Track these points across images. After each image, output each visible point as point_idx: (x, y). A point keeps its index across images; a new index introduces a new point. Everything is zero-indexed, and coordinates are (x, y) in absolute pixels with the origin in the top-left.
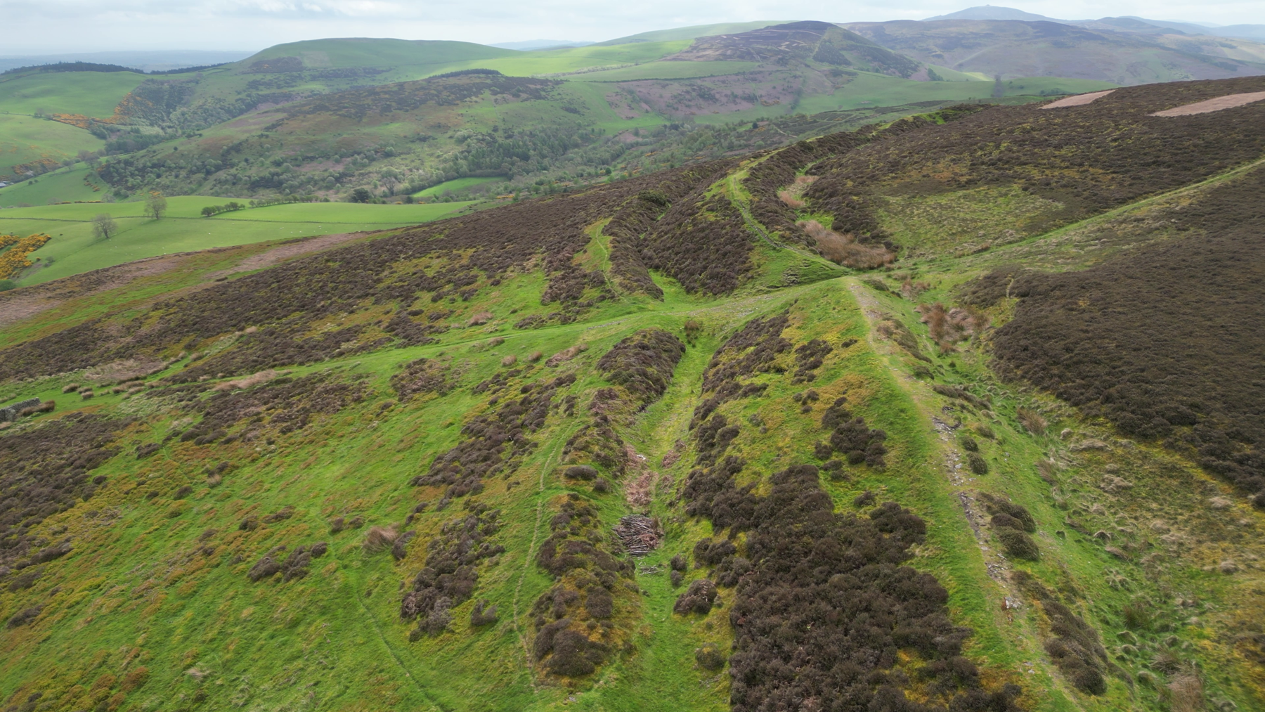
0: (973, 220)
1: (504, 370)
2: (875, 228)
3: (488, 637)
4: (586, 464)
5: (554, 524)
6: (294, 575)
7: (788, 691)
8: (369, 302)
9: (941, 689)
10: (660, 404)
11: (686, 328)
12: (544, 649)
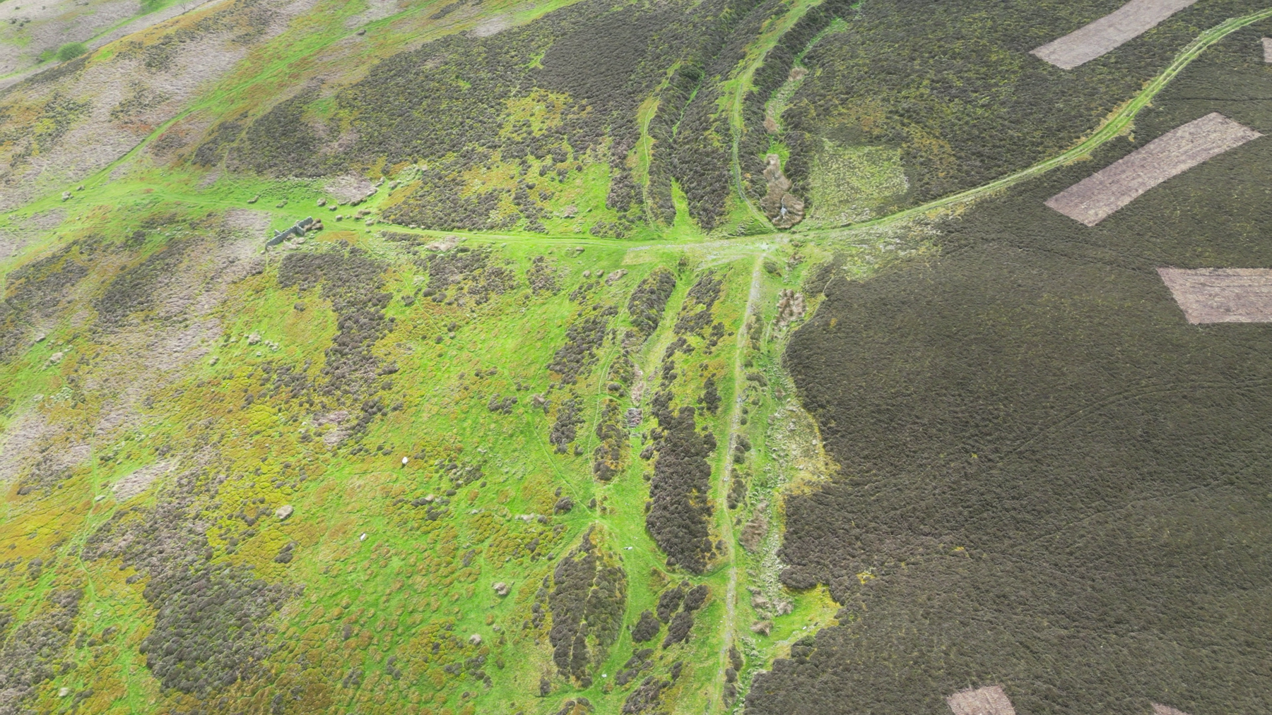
0: (857, 191)
1: (585, 280)
2: (806, 177)
3: (580, 459)
4: (616, 383)
5: (603, 415)
6: (507, 412)
7: (664, 494)
8: (496, 155)
9: (698, 503)
10: (654, 335)
11: (680, 264)
12: (597, 469)
